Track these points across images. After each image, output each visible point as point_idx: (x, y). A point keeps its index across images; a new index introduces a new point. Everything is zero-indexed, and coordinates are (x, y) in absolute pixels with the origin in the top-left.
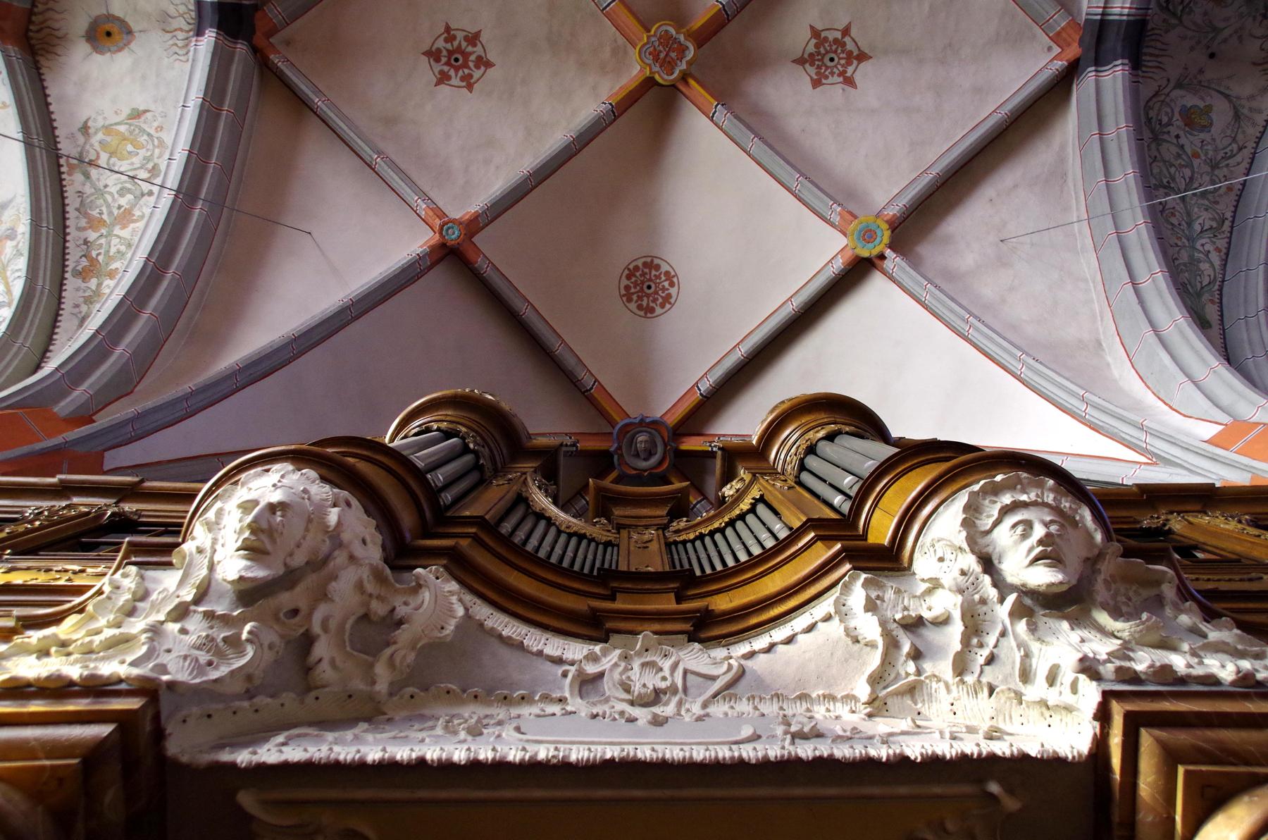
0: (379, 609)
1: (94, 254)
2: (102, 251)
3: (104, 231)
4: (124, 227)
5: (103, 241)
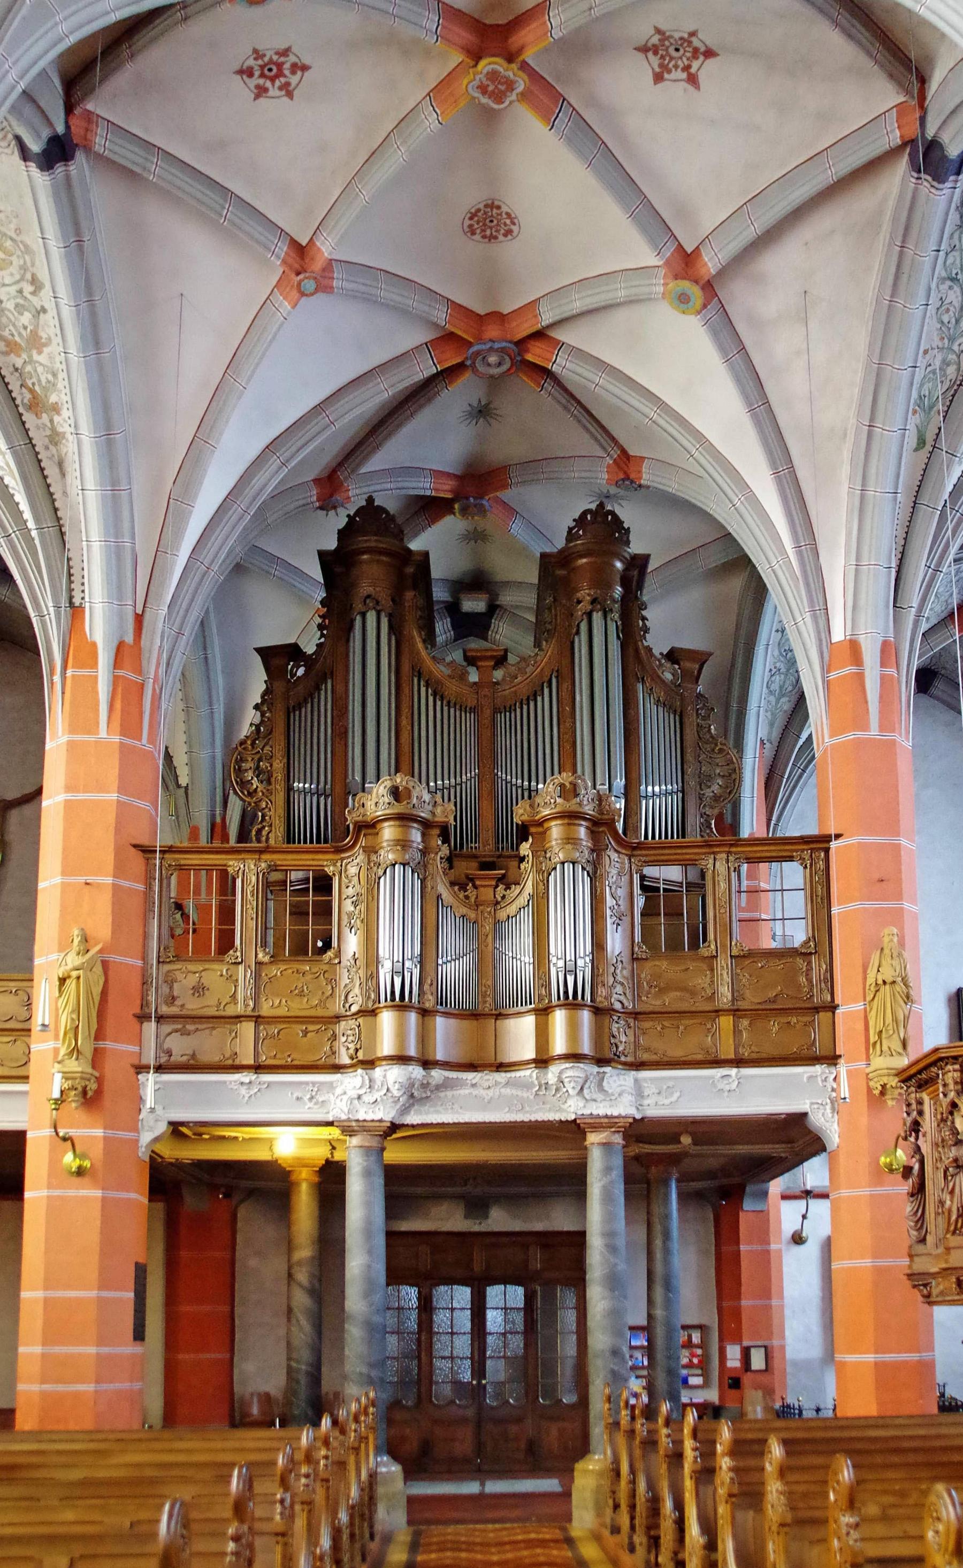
0: (425, 1082)
1: (29, 383)
2: (34, 380)
3: (24, 356)
4: (40, 352)
5: (28, 368)
